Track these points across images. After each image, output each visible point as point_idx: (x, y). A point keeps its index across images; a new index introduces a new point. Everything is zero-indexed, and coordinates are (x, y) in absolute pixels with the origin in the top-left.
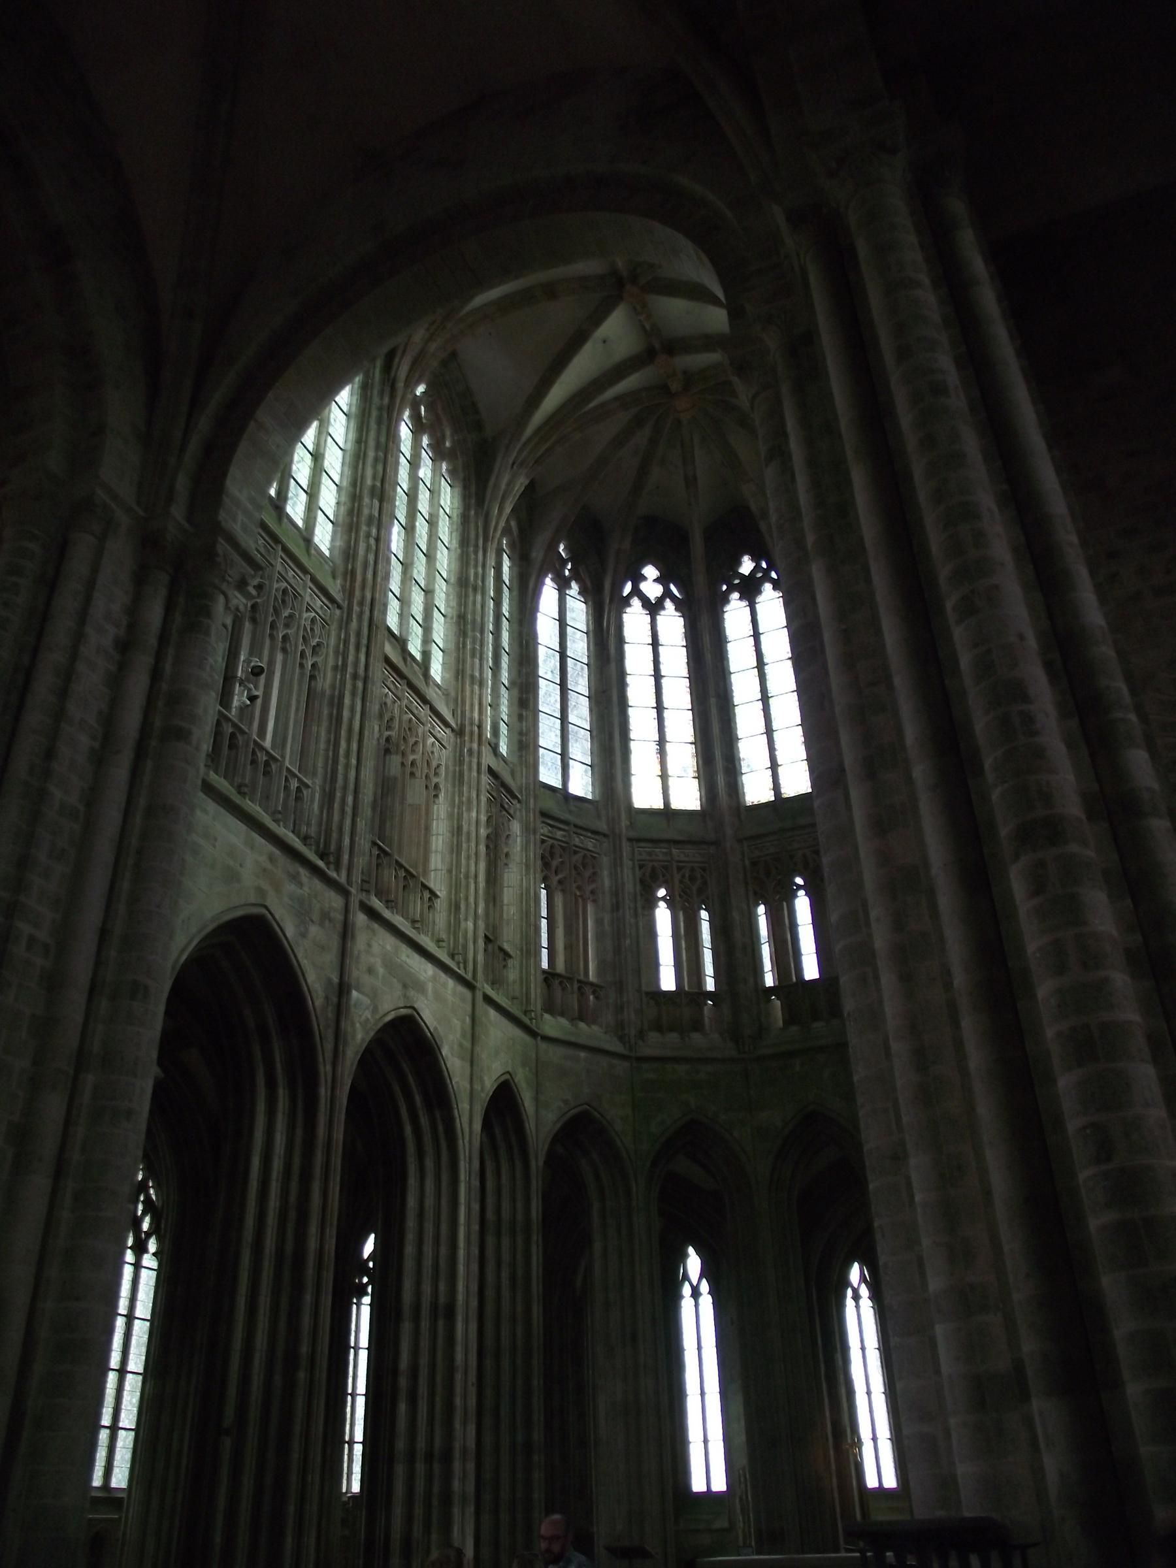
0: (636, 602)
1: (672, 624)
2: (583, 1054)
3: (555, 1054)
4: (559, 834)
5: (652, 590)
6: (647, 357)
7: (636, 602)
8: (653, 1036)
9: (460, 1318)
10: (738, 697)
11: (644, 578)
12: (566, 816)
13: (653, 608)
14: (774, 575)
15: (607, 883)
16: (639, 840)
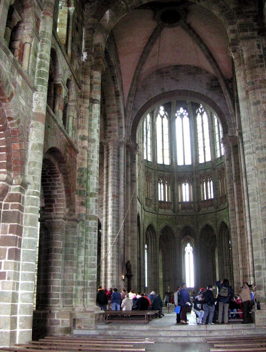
1: (166, 121)
2: (151, 214)
3: (147, 213)
7: (159, 115)
8: (160, 209)
13: (162, 117)
14: (187, 114)
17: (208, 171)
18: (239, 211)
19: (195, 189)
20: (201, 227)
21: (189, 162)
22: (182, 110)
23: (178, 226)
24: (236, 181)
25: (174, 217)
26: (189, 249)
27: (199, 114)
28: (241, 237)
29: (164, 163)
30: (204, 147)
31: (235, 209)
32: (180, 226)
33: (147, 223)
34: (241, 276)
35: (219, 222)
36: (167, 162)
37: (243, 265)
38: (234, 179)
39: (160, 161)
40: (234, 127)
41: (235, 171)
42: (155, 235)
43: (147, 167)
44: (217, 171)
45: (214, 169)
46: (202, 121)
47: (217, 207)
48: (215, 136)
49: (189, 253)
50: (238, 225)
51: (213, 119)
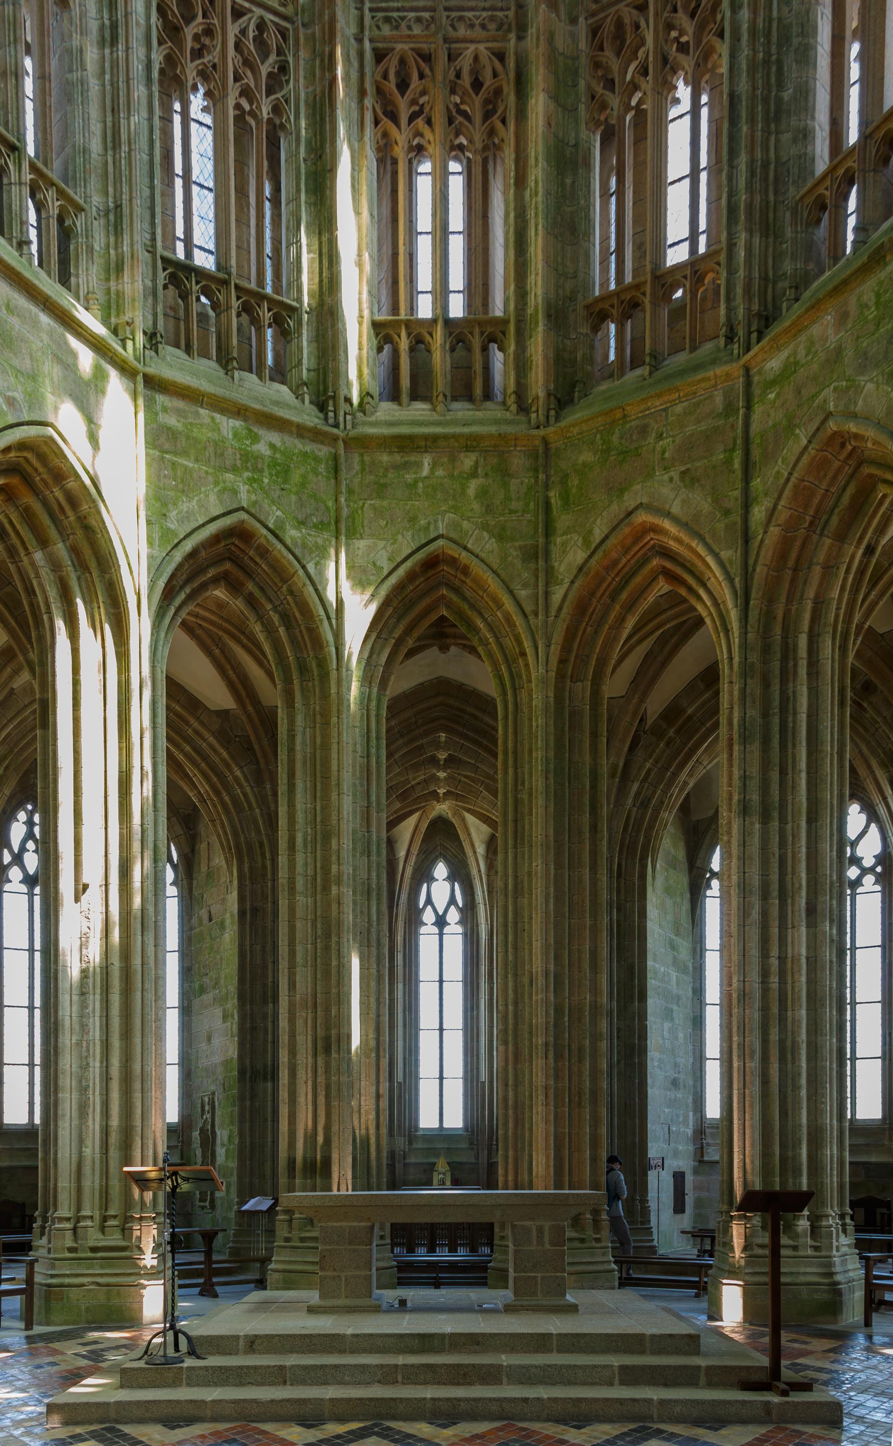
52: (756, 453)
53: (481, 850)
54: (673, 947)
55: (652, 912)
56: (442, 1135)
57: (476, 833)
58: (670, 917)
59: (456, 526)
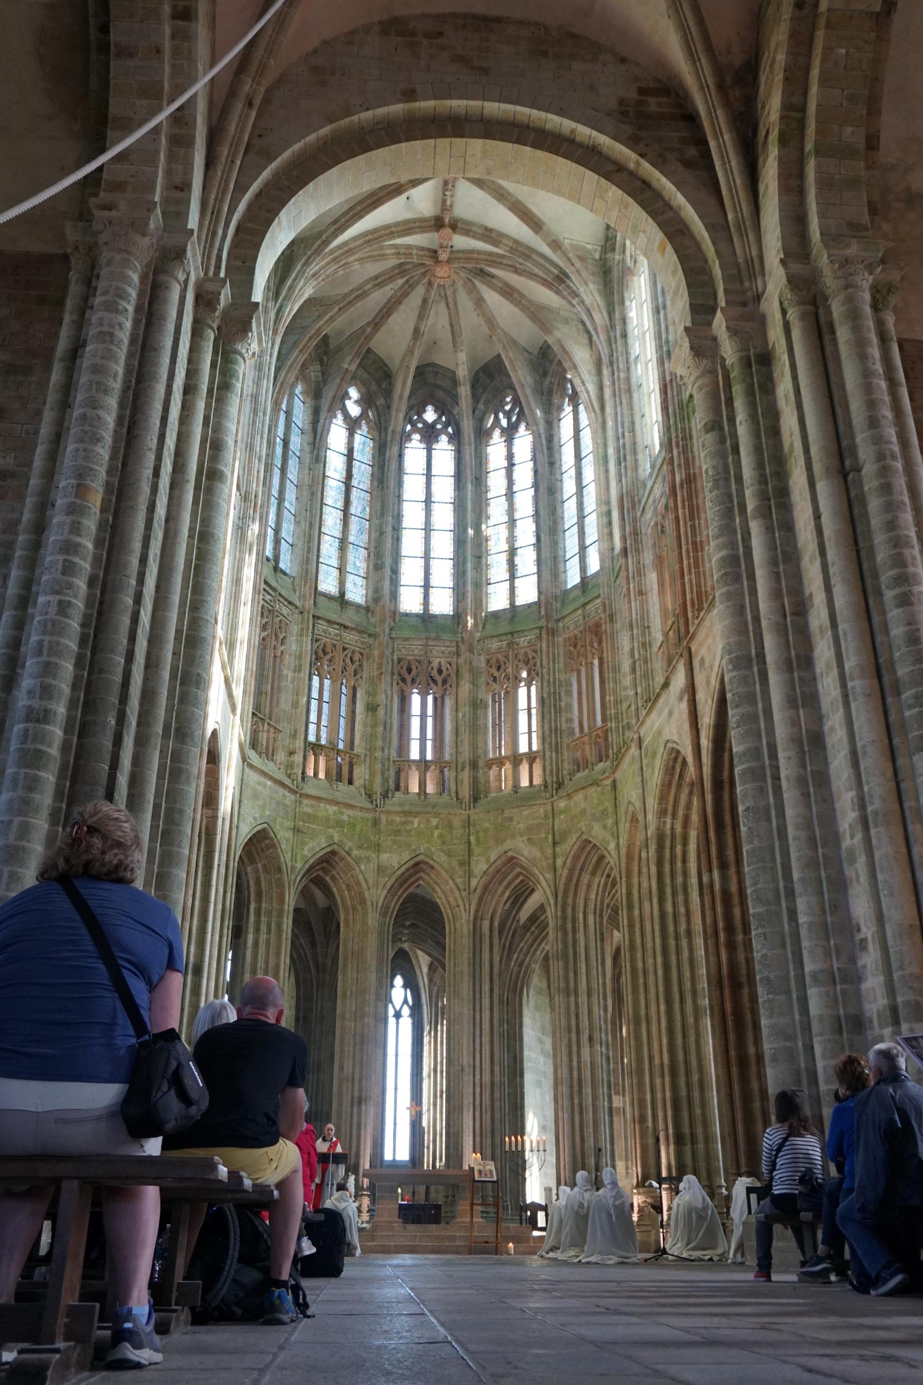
0: (340, 416)
1: (363, 443)
2: (269, 783)
4: (268, 597)
5: (354, 410)
6: (437, 223)
9: (205, 975)
10: (406, 523)
11: (350, 398)
12: (274, 584)
14: (450, 430)
15: (294, 647)
16: (319, 618)
17: (523, 641)
18: (788, 661)
19: (465, 710)
20: (480, 866)
21: (442, 604)
22: (430, 415)
23: (384, 857)
24: (764, 512)
25: (370, 816)
26: (399, 993)
27: (497, 433)
28: (806, 795)
29: (342, 594)
30: (512, 552)
31: (761, 656)
32: (395, 859)
33: (250, 820)
34: (816, 1027)
35: (569, 845)
36: (356, 593)
37: (827, 953)
38: (751, 505)
39: (328, 584)
40: (752, 277)
41: (760, 465)
42: (280, 885)
43: (274, 590)
44: (561, 640)
45: (552, 633)
46: (510, 457)
47: (560, 785)
48: (559, 510)
49: (398, 1015)
50: (781, 732)
51: (556, 447)
52: (557, 838)
53: (425, 970)
54: (541, 1042)
55: (527, 1021)
56: (394, 1164)
57: (423, 961)
58: (538, 1024)
59: (428, 849)
